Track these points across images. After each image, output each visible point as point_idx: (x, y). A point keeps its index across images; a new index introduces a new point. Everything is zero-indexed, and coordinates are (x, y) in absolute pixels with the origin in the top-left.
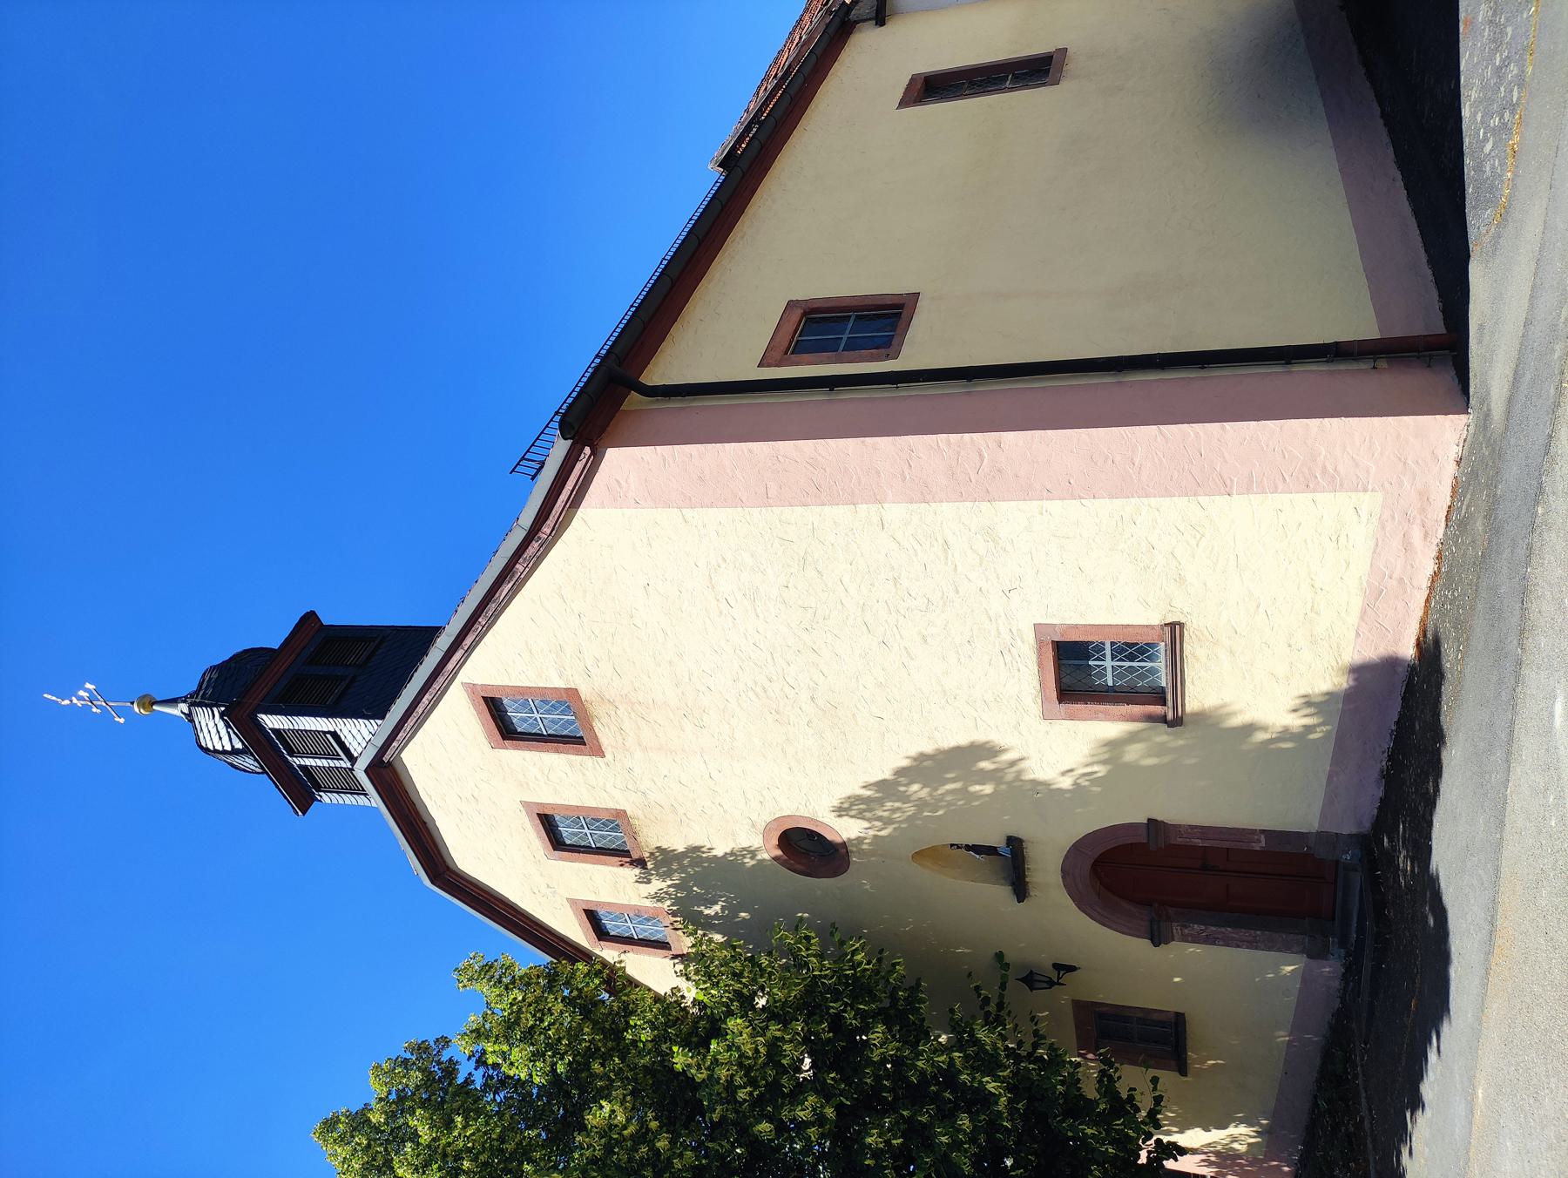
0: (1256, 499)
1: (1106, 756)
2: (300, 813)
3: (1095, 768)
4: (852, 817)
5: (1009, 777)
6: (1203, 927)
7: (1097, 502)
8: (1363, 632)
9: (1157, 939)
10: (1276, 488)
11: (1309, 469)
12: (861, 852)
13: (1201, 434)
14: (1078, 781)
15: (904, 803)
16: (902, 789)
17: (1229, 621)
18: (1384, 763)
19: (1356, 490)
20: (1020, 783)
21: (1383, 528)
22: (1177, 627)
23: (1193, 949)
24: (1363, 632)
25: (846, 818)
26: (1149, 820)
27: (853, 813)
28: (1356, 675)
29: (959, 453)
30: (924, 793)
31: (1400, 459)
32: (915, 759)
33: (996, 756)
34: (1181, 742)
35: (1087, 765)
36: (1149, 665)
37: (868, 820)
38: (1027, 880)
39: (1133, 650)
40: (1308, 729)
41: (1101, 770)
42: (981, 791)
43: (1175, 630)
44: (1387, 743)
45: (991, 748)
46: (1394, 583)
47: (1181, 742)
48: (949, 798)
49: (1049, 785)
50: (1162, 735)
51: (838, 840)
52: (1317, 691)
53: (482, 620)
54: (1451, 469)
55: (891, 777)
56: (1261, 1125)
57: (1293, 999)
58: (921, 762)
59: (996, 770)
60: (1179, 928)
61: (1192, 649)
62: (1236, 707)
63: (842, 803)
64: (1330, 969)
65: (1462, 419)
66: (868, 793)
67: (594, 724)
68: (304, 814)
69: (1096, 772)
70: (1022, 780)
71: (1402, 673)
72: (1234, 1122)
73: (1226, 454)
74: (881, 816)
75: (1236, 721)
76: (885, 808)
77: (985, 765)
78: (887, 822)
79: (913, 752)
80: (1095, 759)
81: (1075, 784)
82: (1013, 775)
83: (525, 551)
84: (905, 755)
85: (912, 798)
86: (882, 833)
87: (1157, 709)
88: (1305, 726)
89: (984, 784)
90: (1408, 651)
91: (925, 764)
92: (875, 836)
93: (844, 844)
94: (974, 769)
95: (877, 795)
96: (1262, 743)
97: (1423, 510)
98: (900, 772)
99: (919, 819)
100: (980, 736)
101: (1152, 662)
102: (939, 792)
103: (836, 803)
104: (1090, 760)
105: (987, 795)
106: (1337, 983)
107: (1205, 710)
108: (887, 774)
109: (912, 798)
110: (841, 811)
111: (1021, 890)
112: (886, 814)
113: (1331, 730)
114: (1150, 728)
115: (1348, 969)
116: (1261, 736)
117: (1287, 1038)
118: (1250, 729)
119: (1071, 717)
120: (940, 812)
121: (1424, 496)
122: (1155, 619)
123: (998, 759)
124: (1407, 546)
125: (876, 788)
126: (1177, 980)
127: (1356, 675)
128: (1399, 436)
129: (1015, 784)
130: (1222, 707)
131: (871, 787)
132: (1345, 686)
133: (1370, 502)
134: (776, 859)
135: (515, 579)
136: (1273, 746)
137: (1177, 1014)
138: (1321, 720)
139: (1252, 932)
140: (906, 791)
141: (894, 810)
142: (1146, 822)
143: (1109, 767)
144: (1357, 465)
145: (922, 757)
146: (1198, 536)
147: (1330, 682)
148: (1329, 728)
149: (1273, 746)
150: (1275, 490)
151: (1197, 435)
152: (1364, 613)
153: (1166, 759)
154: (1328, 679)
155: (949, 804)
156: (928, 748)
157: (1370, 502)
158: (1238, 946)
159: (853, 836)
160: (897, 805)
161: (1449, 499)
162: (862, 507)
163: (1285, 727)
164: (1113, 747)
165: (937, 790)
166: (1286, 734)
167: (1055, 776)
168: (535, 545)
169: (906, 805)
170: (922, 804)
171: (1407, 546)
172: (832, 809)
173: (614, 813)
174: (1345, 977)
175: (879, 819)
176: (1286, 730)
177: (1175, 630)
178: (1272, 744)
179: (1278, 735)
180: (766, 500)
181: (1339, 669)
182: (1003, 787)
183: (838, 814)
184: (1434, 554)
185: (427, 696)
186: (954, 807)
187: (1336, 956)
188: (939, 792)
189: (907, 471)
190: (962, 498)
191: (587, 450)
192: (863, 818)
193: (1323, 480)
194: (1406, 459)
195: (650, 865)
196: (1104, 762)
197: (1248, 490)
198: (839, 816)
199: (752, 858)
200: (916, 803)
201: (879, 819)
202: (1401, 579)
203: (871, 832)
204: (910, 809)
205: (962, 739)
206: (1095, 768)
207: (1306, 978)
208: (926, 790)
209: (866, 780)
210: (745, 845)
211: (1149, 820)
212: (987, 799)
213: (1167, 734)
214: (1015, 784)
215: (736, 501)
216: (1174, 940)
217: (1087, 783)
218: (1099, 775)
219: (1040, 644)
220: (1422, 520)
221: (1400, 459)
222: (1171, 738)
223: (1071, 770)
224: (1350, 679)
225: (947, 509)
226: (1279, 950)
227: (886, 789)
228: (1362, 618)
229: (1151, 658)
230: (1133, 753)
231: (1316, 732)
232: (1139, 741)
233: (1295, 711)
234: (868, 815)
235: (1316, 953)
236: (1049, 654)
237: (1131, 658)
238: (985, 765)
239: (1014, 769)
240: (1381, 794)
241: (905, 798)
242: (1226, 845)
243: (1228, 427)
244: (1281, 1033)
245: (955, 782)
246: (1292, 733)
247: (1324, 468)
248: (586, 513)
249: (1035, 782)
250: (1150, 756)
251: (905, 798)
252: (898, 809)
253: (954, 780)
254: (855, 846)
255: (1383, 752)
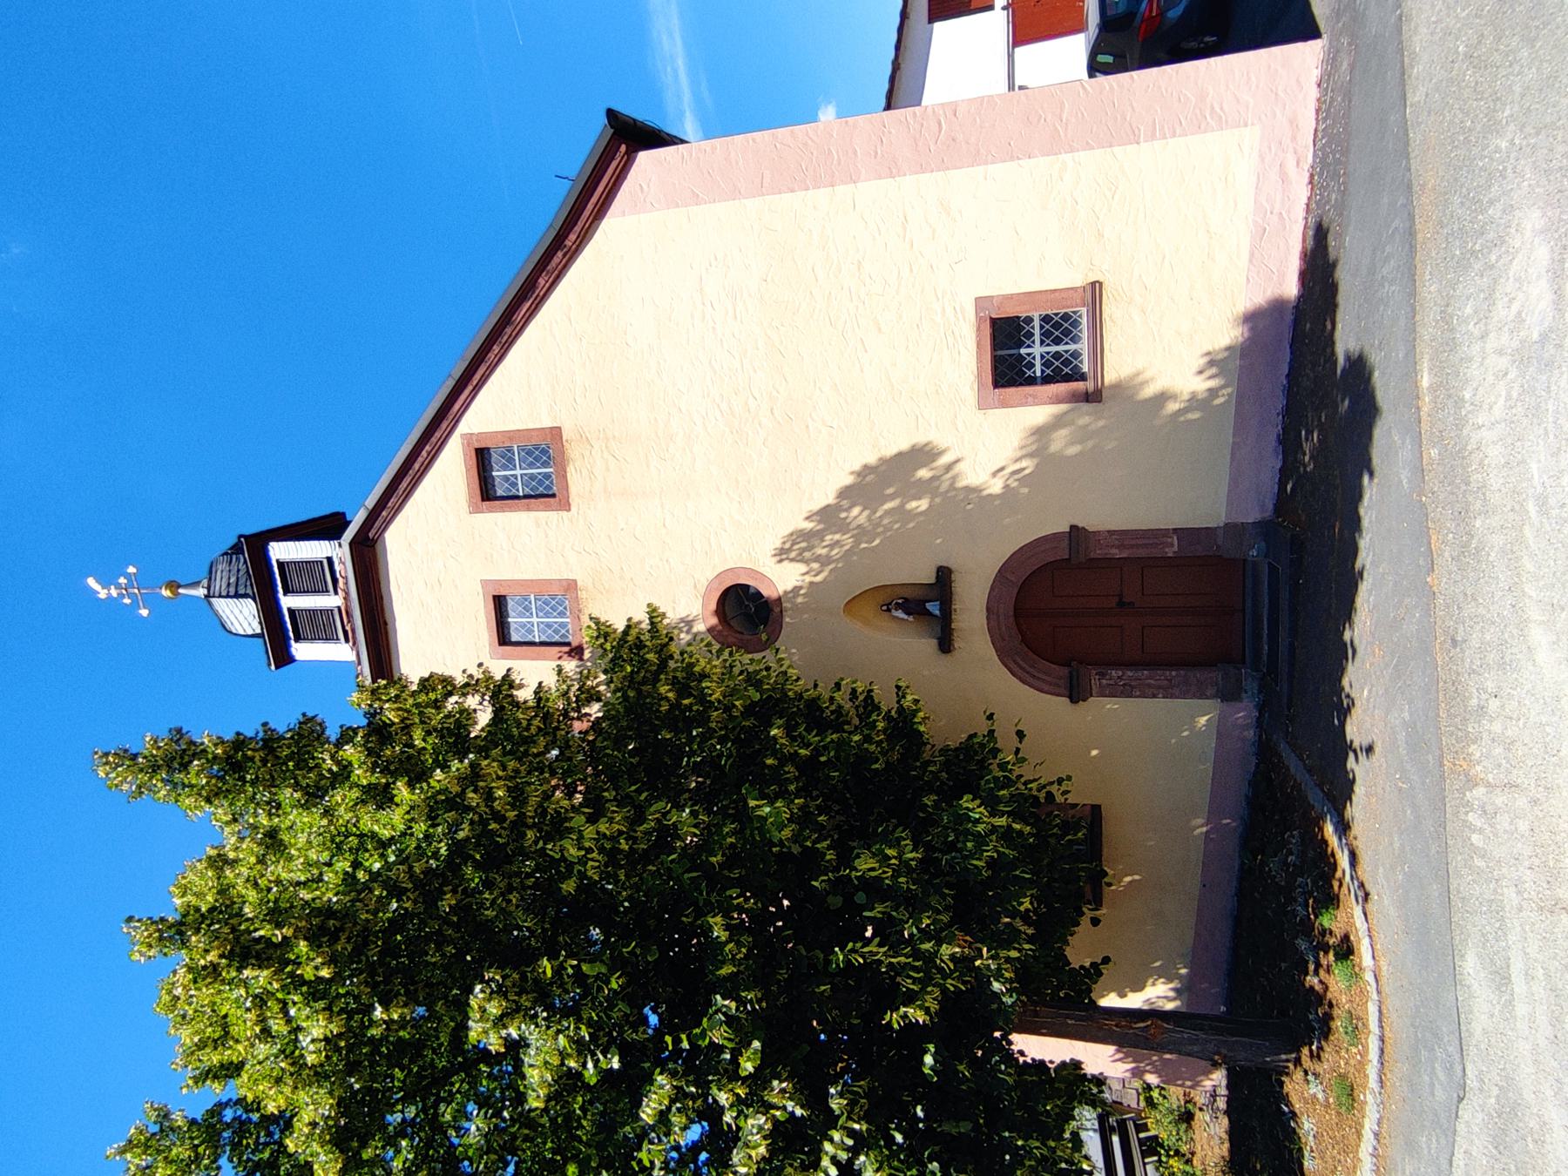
0: (1157, 144)
1: (1034, 447)
2: (273, 667)
3: (1024, 464)
4: (792, 560)
5: (945, 486)
6: (1120, 673)
7: (1032, 161)
8: (1253, 278)
9: (1076, 694)
10: (1175, 132)
11: (1201, 110)
12: (796, 607)
13: (1114, 84)
14: (1009, 482)
15: (844, 534)
16: (843, 515)
17: (1140, 276)
18: (1280, 427)
19: (1239, 126)
20: (954, 493)
21: (1263, 160)
22: (1097, 285)
23: (1111, 705)
24: (1253, 278)
25: (786, 563)
26: (1072, 527)
27: (793, 555)
28: (1250, 325)
29: (922, 125)
30: (862, 519)
31: (1272, 91)
32: (859, 474)
33: (934, 461)
34: (1101, 423)
35: (1016, 461)
36: (1072, 347)
37: (806, 562)
38: (953, 626)
39: (1059, 327)
40: (1213, 392)
41: (1028, 465)
42: (917, 507)
43: (1095, 290)
44: (1280, 403)
45: (933, 449)
46: (1275, 218)
47: (1101, 423)
48: (886, 521)
49: (981, 491)
50: (1086, 416)
51: (774, 595)
52: (1217, 347)
53: (496, 348)
54: (1314, 93)
55: (835, 502)
56: (1180, 977)
57: (1209, 766)
58: (865, 477)
59: (933, 478)
60: (1097, 677)
61: (1109, 309)
62: (1147, 375)
63: (784, 543)
64: (1243, 713)
65: (1318, 42)
66: (809, 525)
67: (568, 470)
68: (277, 668)
69: (1024, 469)
70: (955, 489)
71: (1289, 318)
72: (1151, 976)
73: (1135, 104)
74: (820, 555)
75: (1149, 391)
76: (825, 544)
77: (924, 473)
78: (824, 561)
79: (857, 467)
80: (1024, 452)
81: (1006, 486)
82: (947, 483)
83: (550, 261)
84: (850, 470)
85: (851, 527)
86: (819, 579)
87: (1078, 386)
88: (1210, 390)
89: (920, 499)
90: (1291, 289)
91: (868, 479)
92: (811, 583)
93: (779, 599)
94: (913, 480)
95: (818, 528)
96: (1171, 415)
97: (1294, 139)
98: (844, 493)
99: (854, 554)
100: (920, 439)
101: (1075, 343)
102: (878, 514)
103: (778, 544)
104: (1019, 454)
105: (921, 513)
106: (1252, 732)
107: (1121, 381)
108: (829, 498)
109: (851, 527)
110: (782, 554)
111: (945, 644)
112: (824, 551)
113: (1232, 392)
114: (1072, 410)
115: (1261, 708)
116: (1172, 407)
117: (1204, 829)
118: (1163, 397)
119: (1004, 404)
120: (877, 542)
121: (1293, 123)
122: (1077, 279)
123: (935, 464)
124: (1284, 178)
125: (818, 518)
126: (1094, 753)
127: (1250, 325)
128: (1269, 67)
129: (949, 495)
130: (1138, 374)
131: (814, 518)
132: (1240, 339)
133: (1251, 136)
134: (710, 630)
135: (534, 296)
136: (1182, 419)
137: (1093, 806)
138: (1222, 382)
139: (1168, 673)
140: (847, 518)
141: (832, 546)
142: (1068, 530)
143: (1035, 461)
144: (1238, 101)
145: (867, 470)
146: (1114, 188)
147: (1227, 336)
148: (1229, 390)
149: (1182, 419)
150: (1174, 135)
151: (1111, 87)
152: (1252, 255)
153: (1090, 444)
154: (1226, 334)
155: (887, 529)
156: (871, 459)
157: (1251, 136)
158: (1154, 696)
159: (789, 587)
160: (837, 537)
161: (1314, 122)
162: (840, 189)
163: (1193, 393)
164: (1041, 433)
165: (875, 513)
166: (1194, 402)
167: (987, 478)
168: (560, 254)
169: (846, 537)
170: (861, 533)
171: (1284, 178)
172: (773, 552)
173: (565, 584)
174: (1259, 723)
175: (817, 559)
176: (1193, 397)
177: (1095, 290)
178: (1182, 415)
179: (1187, 404)
180: (760, 190)
181: (1235, 321)
182: (938, 500)
183: (778, 558)
184: (1306, 180)
185: (428, 448)
186: (889, 534)
187: (1250, 693)
188: (878, 514)
189: (879, 147)
190: (922, 169)
191: (623, 148)
192: (803, 561)
193: (1212, 118)
194: (1277, 89)
195: (587, 655)
196: (1031, 455)
197: (1153, 137)
198: (780, 561)
199: (688, 632)
200: (855, 532)
201: (817, 559)
202: (1281, 213)
203: (808, 579)
204: (848, 540)
205: (904, 445)
206: (1024, 464)
207: (1222, 731)
208: (866, 513)
209: (810, 509)
210: (683, 615)
211: (1072, 527)
212: (922, 518)
213: (1089, 414)
214: (949, 495)
215: (735, 194)
216: (1091, 696)
217: (1016, 484)
218: (1027, 472)
219: (980, 320)
220: (1294, 148)
221: (1272, 91)
222: (1093, 418)
223: (1002, 469)
224: (1246, 329)
225: (908, 182)
226: (1194, 696)
227: (828, 517)
228: (1251, 261)
229: (1075, 340)
230: (1059, 441)
231: (1219, 397)
232: (1064, 426)
233: (1201, 372)
234: (807, 555)
235: (1228, 695)
236: (987, 331)
237: (1057, 341)
238: (924, 473)
239: (949, 475)
240: (1279, 465)
241: (843, 527)
242: (1142, 553)
243: (1135, 77)
244: (1200, 821)
245: (893, 499)
246: (1197, 400)
247: (1212, 108)
248: (608, 225)
249: (968, 489)
250: (1072, 444)
251: (843, 527)
252: (838, 542)
253: (892, 497)
254: (789, 600)
255: (1278, 414)
